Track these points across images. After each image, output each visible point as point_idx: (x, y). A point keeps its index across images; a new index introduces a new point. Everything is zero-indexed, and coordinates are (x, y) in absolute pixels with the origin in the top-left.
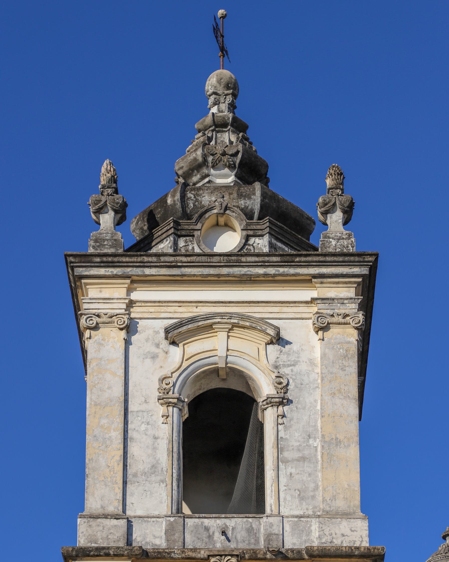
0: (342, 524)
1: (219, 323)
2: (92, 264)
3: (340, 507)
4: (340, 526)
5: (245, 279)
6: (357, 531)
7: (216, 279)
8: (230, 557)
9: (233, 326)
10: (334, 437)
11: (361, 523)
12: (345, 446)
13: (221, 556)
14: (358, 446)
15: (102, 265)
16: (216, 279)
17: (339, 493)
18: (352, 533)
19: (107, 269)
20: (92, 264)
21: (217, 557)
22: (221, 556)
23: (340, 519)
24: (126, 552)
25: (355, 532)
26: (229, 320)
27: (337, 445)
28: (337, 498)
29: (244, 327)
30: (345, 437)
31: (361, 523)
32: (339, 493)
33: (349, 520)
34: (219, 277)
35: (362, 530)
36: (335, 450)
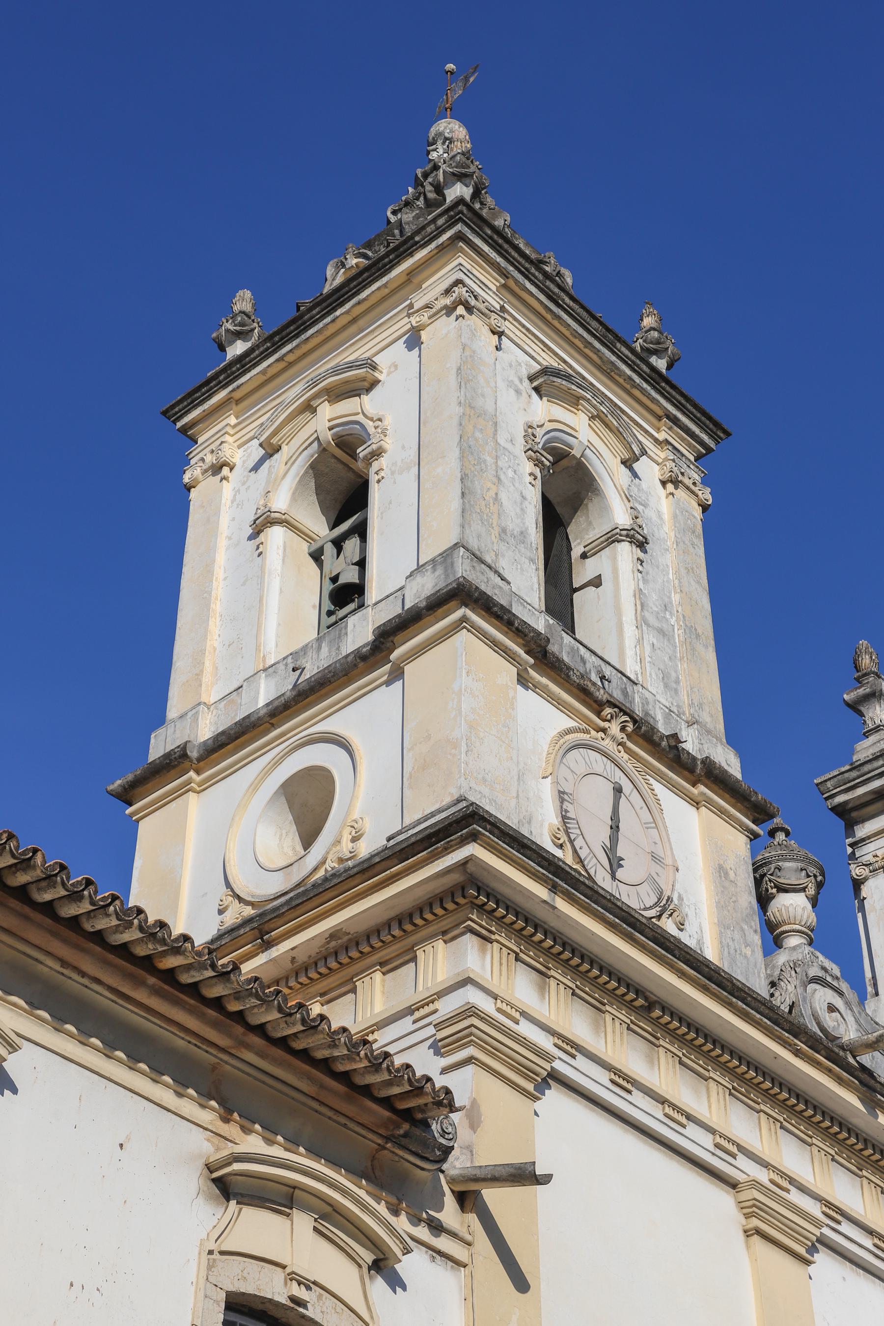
1: (588, 401)
2: (481, 233)
5: (605, 369)
7: (581, 345)
8: (628, 719)
9: (598, 416)
13: (621, 710)
14: (715, 653)
15: (490, 241)
16: (581, 345)
19: (491, 251)
20: (481, 233)
21: (616, 710)
22: (621, 710)
24: (532, 634)
26: (598, 404)
29: (607, 425)
34: (586, 347)
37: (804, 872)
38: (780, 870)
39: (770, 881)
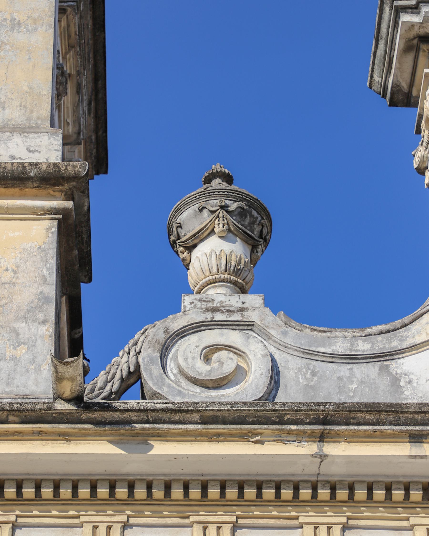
0: (13, 140)
3: (12, 119)
4: (9, 145)
6: (40, 152)
10: (9, 17)
11: (49, 139)
12: (28, 30)
17: (12, 99)
18: (31, 154)
23: (8, 134)
25: (36, 154)
27: (13, 29)
28: (6, 106)
30: (29, 17)
31: (49, 139)
32: (12, 99)
33: (26, 134)
35: (50, 150)
36: (9, 36)
37: (205, 212)
38: (180, 227)
39: (180, 246)
